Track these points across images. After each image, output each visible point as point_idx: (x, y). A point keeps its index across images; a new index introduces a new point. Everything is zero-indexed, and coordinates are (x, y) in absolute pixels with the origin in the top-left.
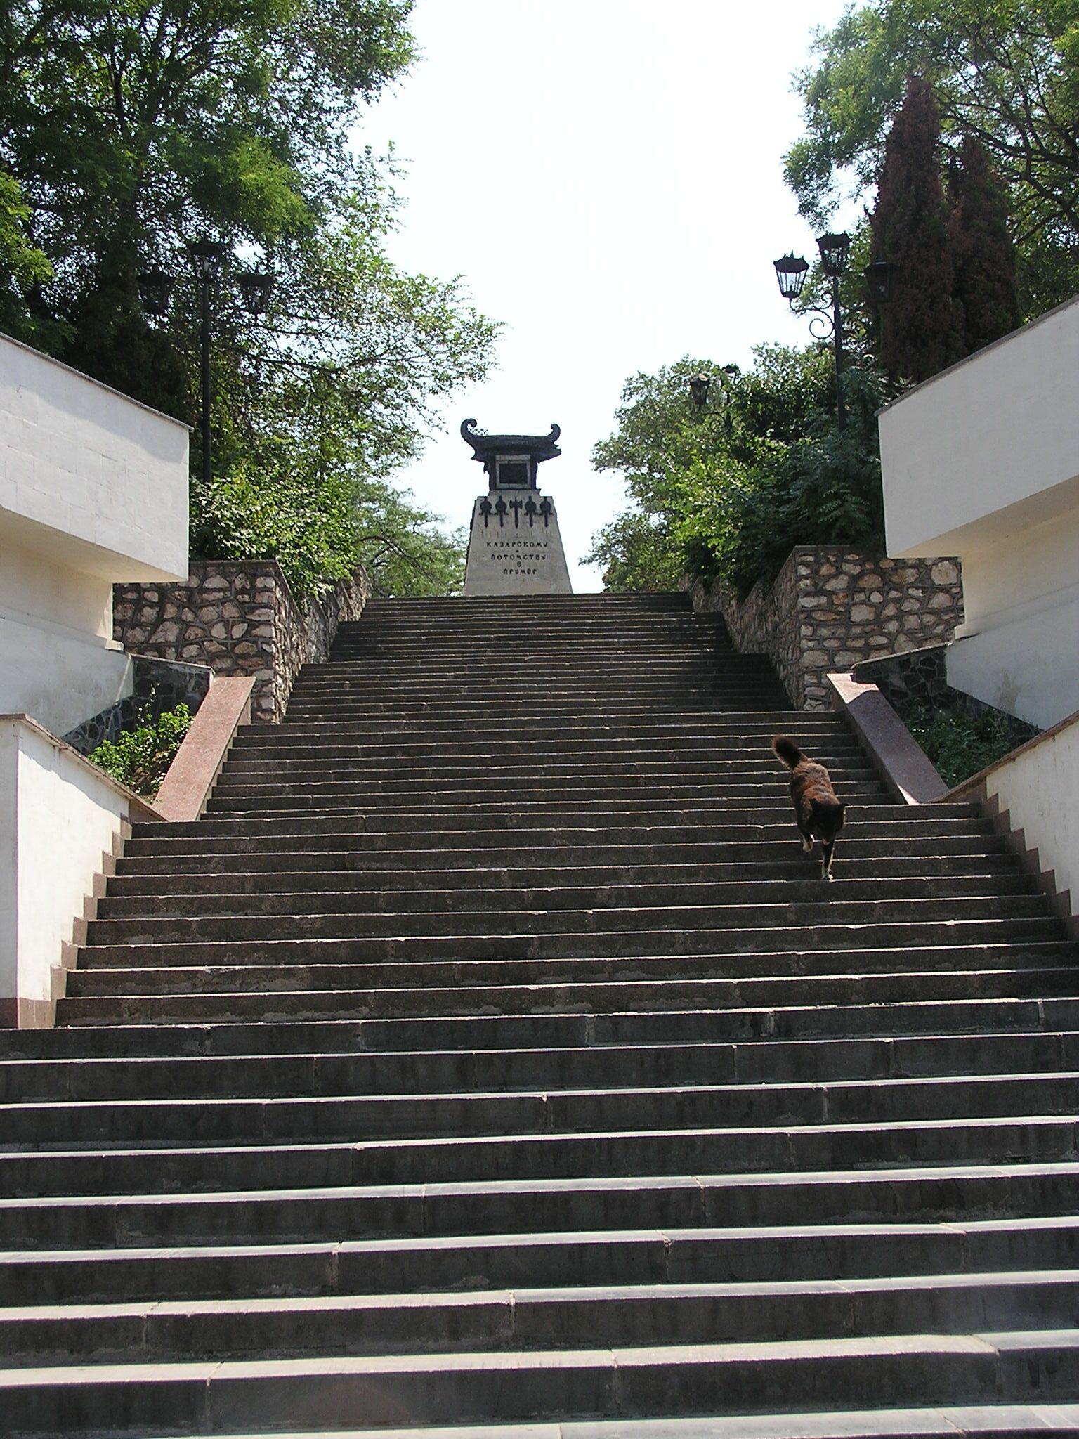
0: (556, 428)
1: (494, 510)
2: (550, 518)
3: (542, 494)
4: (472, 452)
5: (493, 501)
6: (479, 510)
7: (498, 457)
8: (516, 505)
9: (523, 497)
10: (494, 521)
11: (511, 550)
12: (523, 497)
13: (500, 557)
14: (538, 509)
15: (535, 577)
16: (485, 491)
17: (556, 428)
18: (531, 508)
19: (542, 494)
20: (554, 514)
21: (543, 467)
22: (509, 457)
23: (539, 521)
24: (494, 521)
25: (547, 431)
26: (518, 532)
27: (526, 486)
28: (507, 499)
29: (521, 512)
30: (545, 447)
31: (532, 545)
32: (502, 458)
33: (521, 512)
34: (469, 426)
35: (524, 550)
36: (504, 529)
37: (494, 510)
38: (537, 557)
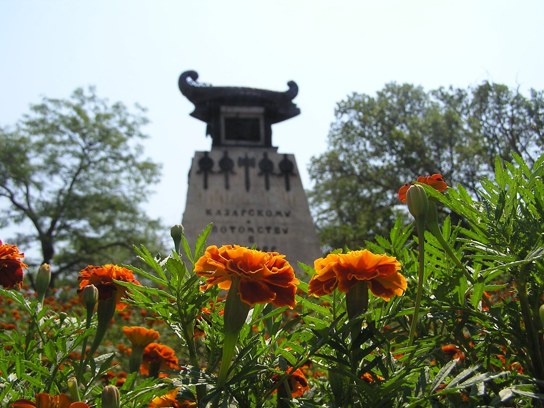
0: (293, 87)
1: (216, 168)
2: (292, 181)
3: (281, 151)
4: (191, 107)
5: (217, 157)
6: (197, 168)
7: (223, 109)
10: (216, 182)
11: (241, 221)
12: (256, 155)
14: (276, 169)
16: (206, 144)
17: (293, 87)
18: (266, 168)
19: (281, 151)
24: (216, 182)
25: (284, 88)
27: (260, 143)
29: (254, 171)
30: (281, 105)
31: (269, 214)
32: (228, 111)
34: (189, 79)
37: (216, 168)
38: (277, 231)
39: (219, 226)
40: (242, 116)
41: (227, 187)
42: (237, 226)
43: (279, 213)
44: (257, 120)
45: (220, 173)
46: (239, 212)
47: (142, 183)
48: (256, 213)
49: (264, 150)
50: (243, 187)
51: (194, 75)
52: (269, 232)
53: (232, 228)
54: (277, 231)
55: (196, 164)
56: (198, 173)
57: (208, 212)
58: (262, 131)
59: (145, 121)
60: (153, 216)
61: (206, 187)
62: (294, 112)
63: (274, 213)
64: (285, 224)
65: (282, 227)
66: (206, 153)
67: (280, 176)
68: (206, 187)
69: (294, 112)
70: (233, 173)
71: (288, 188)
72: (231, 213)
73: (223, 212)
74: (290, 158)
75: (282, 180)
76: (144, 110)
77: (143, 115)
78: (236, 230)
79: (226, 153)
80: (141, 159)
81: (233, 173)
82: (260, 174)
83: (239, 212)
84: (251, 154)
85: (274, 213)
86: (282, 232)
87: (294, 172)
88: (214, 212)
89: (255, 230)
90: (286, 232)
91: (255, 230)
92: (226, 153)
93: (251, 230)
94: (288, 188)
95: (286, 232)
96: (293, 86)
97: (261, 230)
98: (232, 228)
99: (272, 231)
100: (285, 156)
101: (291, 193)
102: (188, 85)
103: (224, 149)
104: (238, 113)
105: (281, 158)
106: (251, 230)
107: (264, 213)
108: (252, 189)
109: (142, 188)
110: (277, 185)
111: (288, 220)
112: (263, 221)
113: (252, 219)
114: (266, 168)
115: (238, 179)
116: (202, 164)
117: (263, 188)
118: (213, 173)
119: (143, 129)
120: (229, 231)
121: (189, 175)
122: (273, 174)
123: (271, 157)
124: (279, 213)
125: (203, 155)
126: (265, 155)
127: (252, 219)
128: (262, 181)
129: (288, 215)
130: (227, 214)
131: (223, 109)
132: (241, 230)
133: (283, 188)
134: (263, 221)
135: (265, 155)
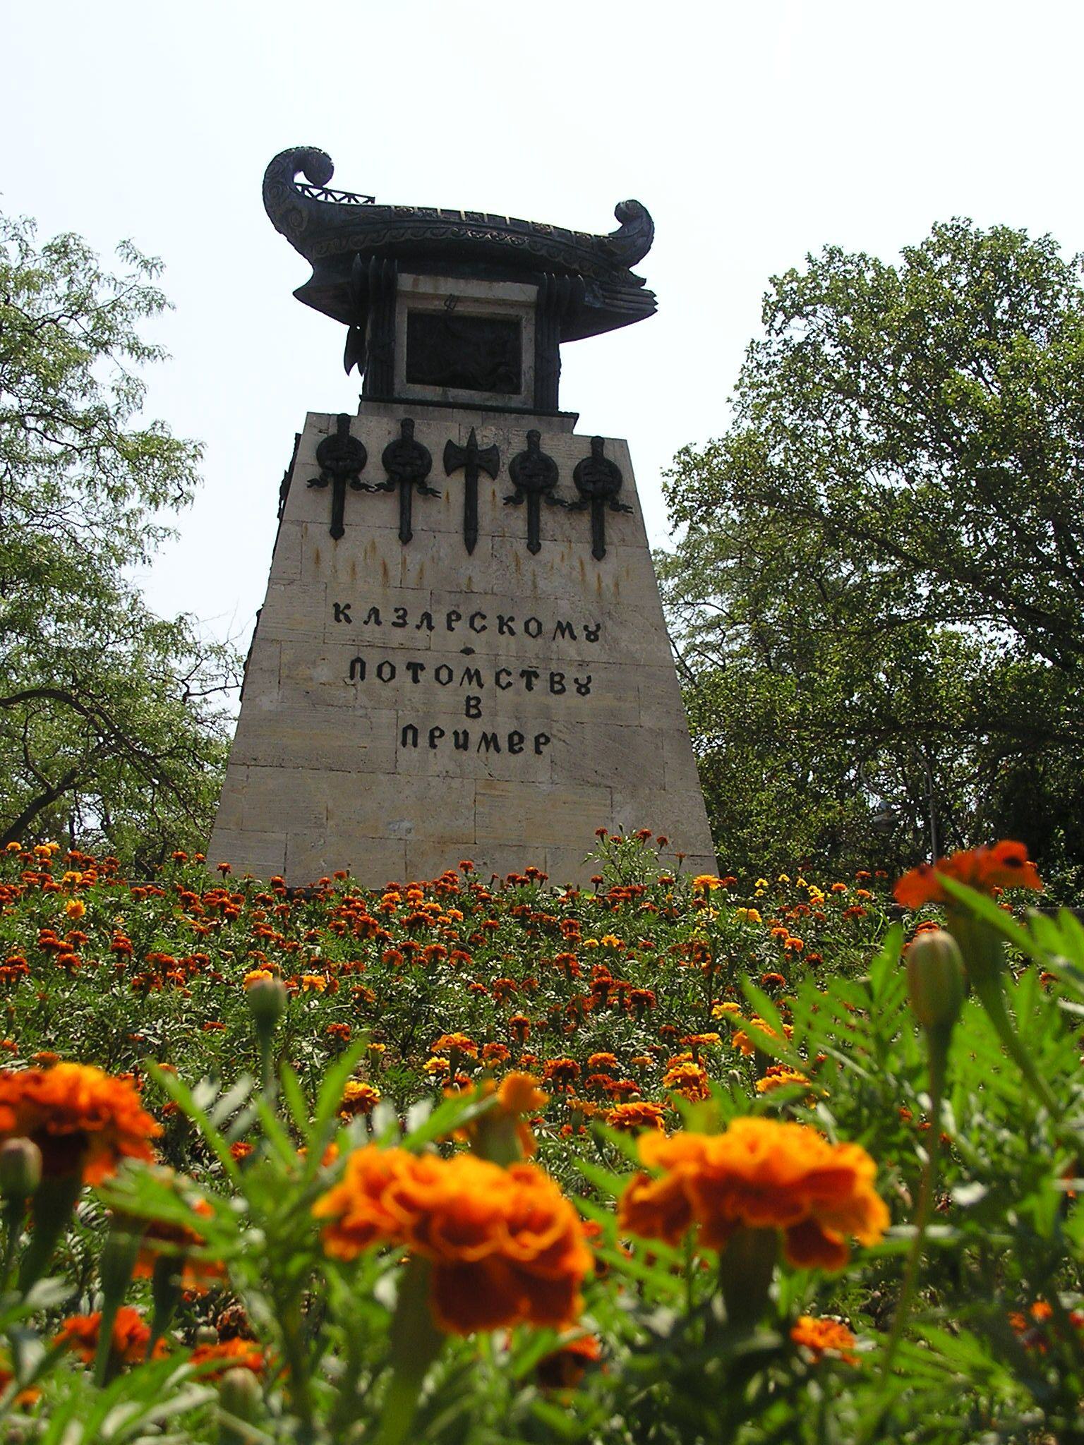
0: (636, 224)
1: (374, 472)
2: (615, 528)
4: (302, 271)
5: (376, 437)
7: (406, 281)
8: (470, 462)
9: (504, 437)
10: (372, 516)
11: (443, 645)
12: (504, 437)
13: (386, 672)
15: (542, 763)
16: (343, 393)
17: (636, 224)
18: (534, 480)
20: (630, 510)
21: (578, 358)
22: (449, 286)
23: (565, 537)
24: (372, 516)
25: (607, 225)
26: (480, 572)
27: (516, 401)
28: (436, 435)
29: (493, 490)
31: (535, 629)
33: (493, 490)
34: (300, 178)
35: (496, 649)
36: (414, 557)
37: (374, 472)
39: (372, 659)
40: (460, 308)
41: (406, 536)
42: (430, 662)
43: (564, 628)
44: (513, 325)
45: (385, 487)
46: (439, 619)
47: (133, 502)
48: (492, 623)
49: (531, 422)
50: (458, 539)
51: (316, 164)
52: (529, 687)
53: (415, 668)
54: (556, 684)
55: (309, 455)
56: (313, 483)
57: (340, 613)
58: (528, 360)
59: (154, 302)
60: (164, 612)
61: (337, 531)
62: (638, 305)
63: (549, 626)
64: (582, 664)
65: (571, 673)
66: (344, 419)
67: (575, 508)
68: (337, 531)
69: (638, 305)
70: (431, 493)
71: (599, 552)
72: (413, 620)
73: (388, 616)
74: (609, 454)
75: (584, 523)
76: (145, 264)
77: (145, 281)
78: (426, 676)
79: (407, 425)
80: (132, 425)
81: (431, 493)
82: (511, 501)
83: (439, 619)
84: (487, 436)
85: (549, 626)
86: (571, 688)
87: (623, 499)
88: (359, 612)
89: (488, 678)
90: (583, 689)
91: (488, 678)
92: (407, 425)
93: (473, 675)
94: (599, 552)
95: (583, 689)
96: (634, 218)
97: (504, 679)
98: (415, 668)
99: (540, 684)
100: (597, 442)
101: (609, 566)
102: (296, 191)
103: (401, 411)
104: (452, 299)
105: (585, 452)
106: (473, 675)
107: (518, 626)
108: (484, 544)
109: (131, 516)
110: (565, 537)
111: (593, 651)
112: (513, 650)
113: (479, 642)
114: (534, 480)
115: (441, 512)
116: (329, 458)
117: (521, 546)
118: (359, 486)
119: (145, 328)
120: (404, 677)
121: (285, 490)
122: (555, 503)
123: (551, 446)
124: (564, 628)
125: (333, 430)
126: (533, 438)
127: (479, 642)
128: (518, 521)
129: (592, 636)
130: (401, 624)
131: (406, 281)
132: (443, 675)
133: (585, 550)
134: (513, 650)
135: (533, 438)
